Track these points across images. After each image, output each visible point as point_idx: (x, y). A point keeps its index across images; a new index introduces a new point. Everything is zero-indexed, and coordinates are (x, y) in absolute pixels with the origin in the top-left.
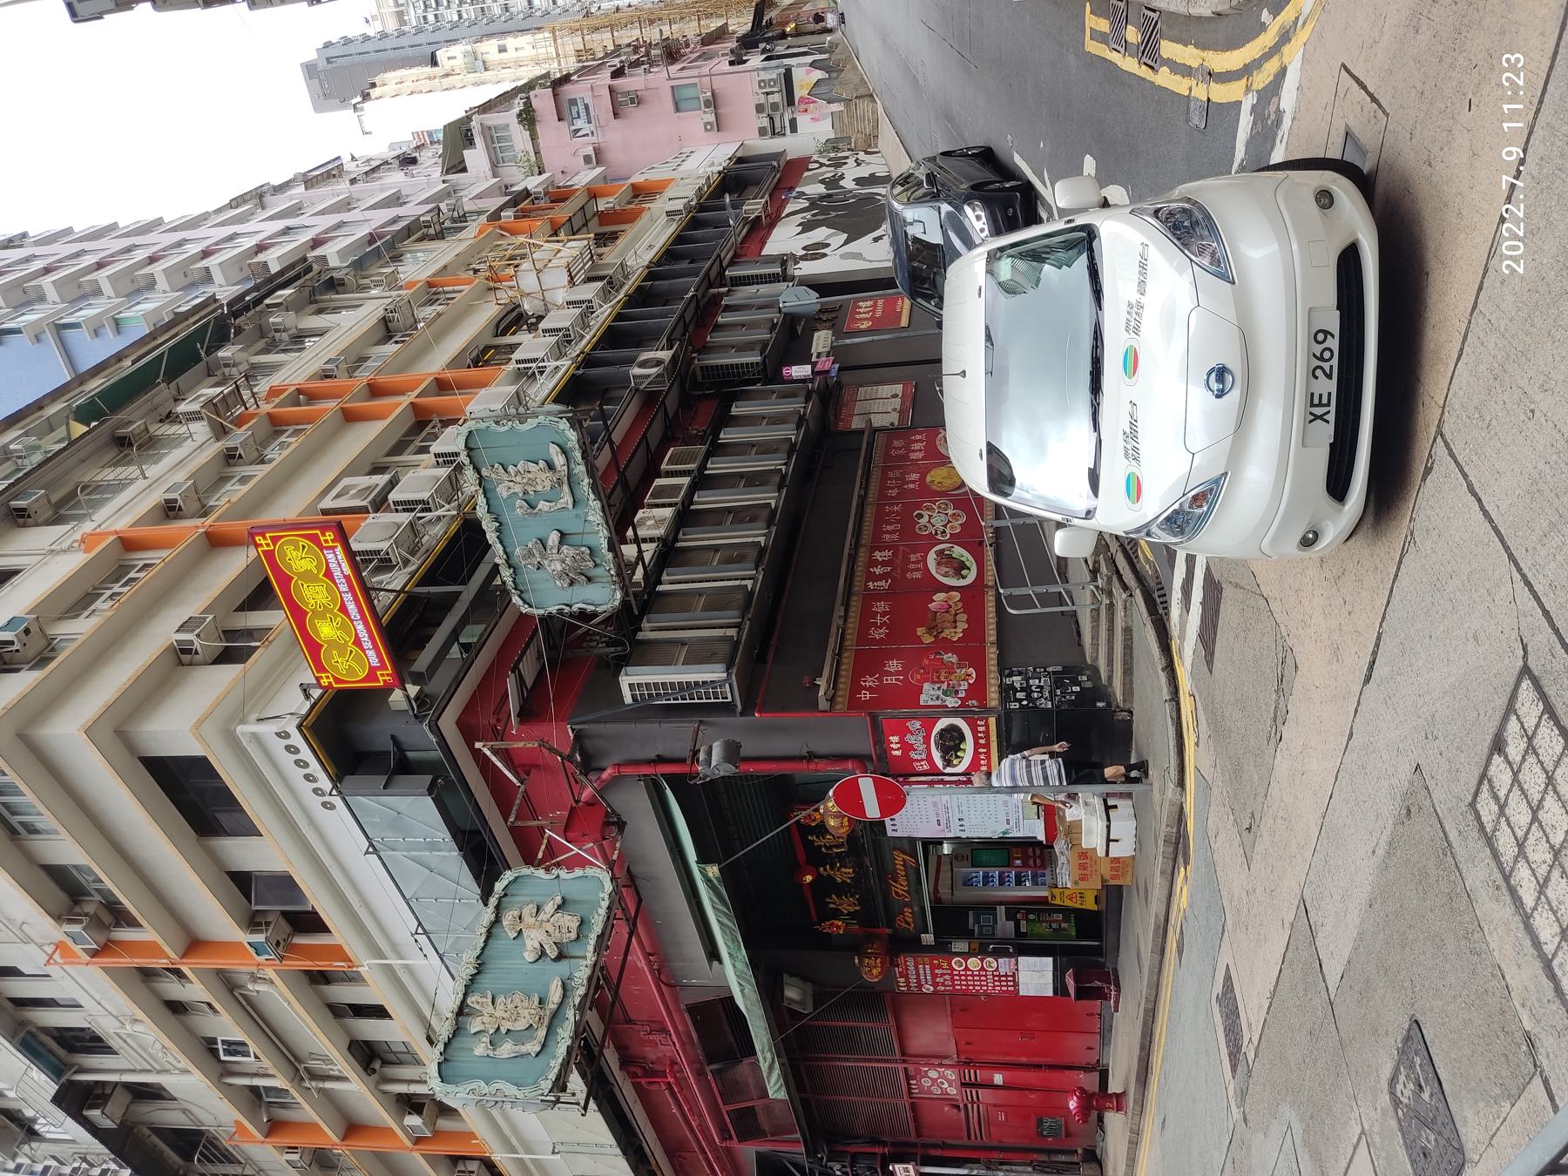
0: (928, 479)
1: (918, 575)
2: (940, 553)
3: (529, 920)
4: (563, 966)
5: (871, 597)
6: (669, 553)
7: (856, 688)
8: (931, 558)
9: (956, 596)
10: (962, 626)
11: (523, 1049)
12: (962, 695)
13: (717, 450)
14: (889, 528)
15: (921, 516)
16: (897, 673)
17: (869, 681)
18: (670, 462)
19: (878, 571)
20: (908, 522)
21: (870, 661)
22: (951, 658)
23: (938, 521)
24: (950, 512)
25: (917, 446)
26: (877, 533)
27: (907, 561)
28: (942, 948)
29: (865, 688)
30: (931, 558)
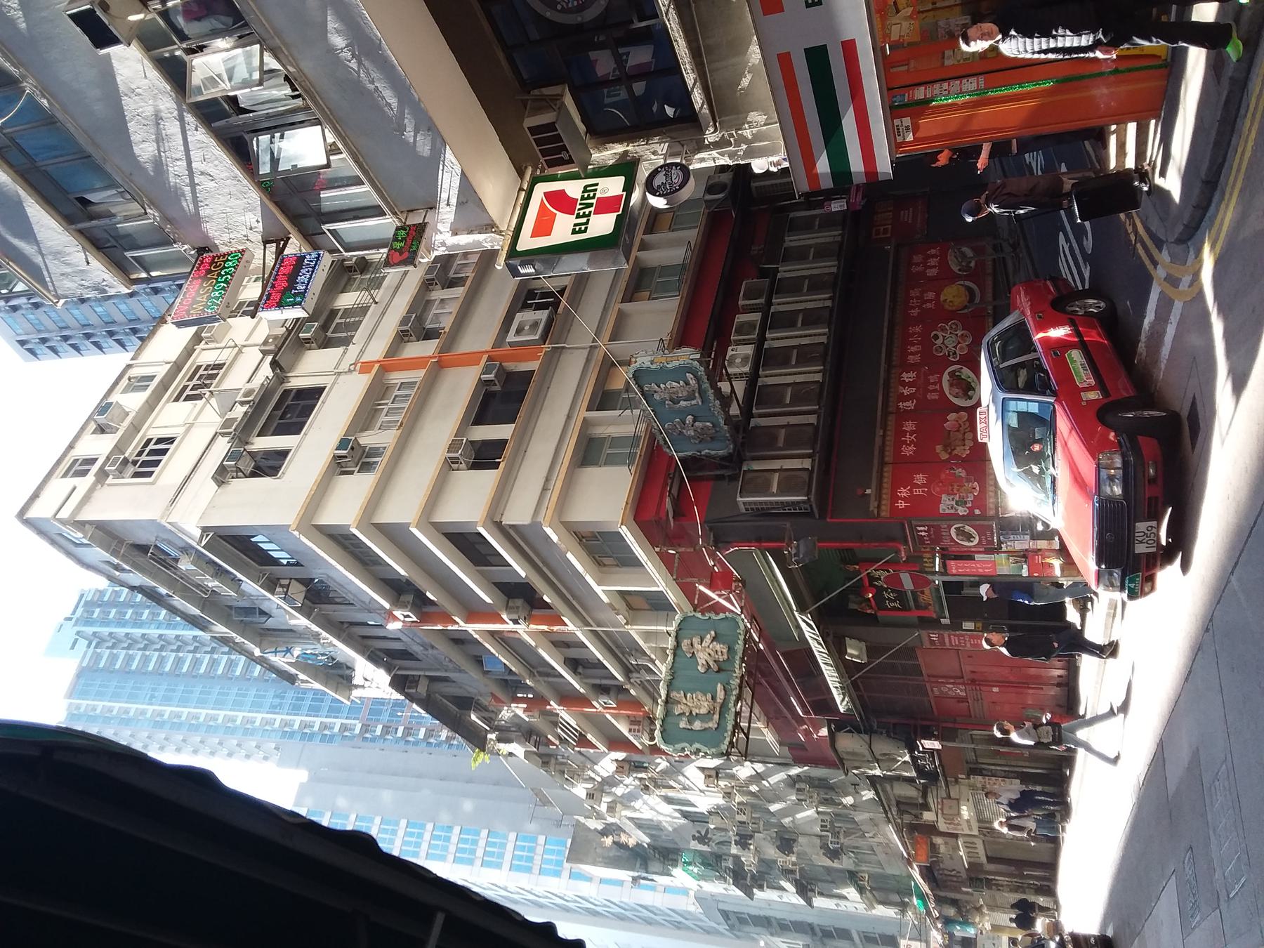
0: (942, 298)
1: (935, 396)
2: (952, 374)
3: (697, 646)
4: (722, 675)
6: (756, 394)
7: (895, 498)
8: (946, 377)
11: (706, 726)
13: (778, 287)
14: (913, 349)
15: (936, 337)
16: (923, 486)
17: (903, 493)
18: (746, 297)
19: (906, 392)
20: (927, 342)
22: (961, 472)
23: (950, 343)
25: (933, 262)
26: (905, 354)
27: (928, 383)
28: (956, 626)
30: (946, 377)
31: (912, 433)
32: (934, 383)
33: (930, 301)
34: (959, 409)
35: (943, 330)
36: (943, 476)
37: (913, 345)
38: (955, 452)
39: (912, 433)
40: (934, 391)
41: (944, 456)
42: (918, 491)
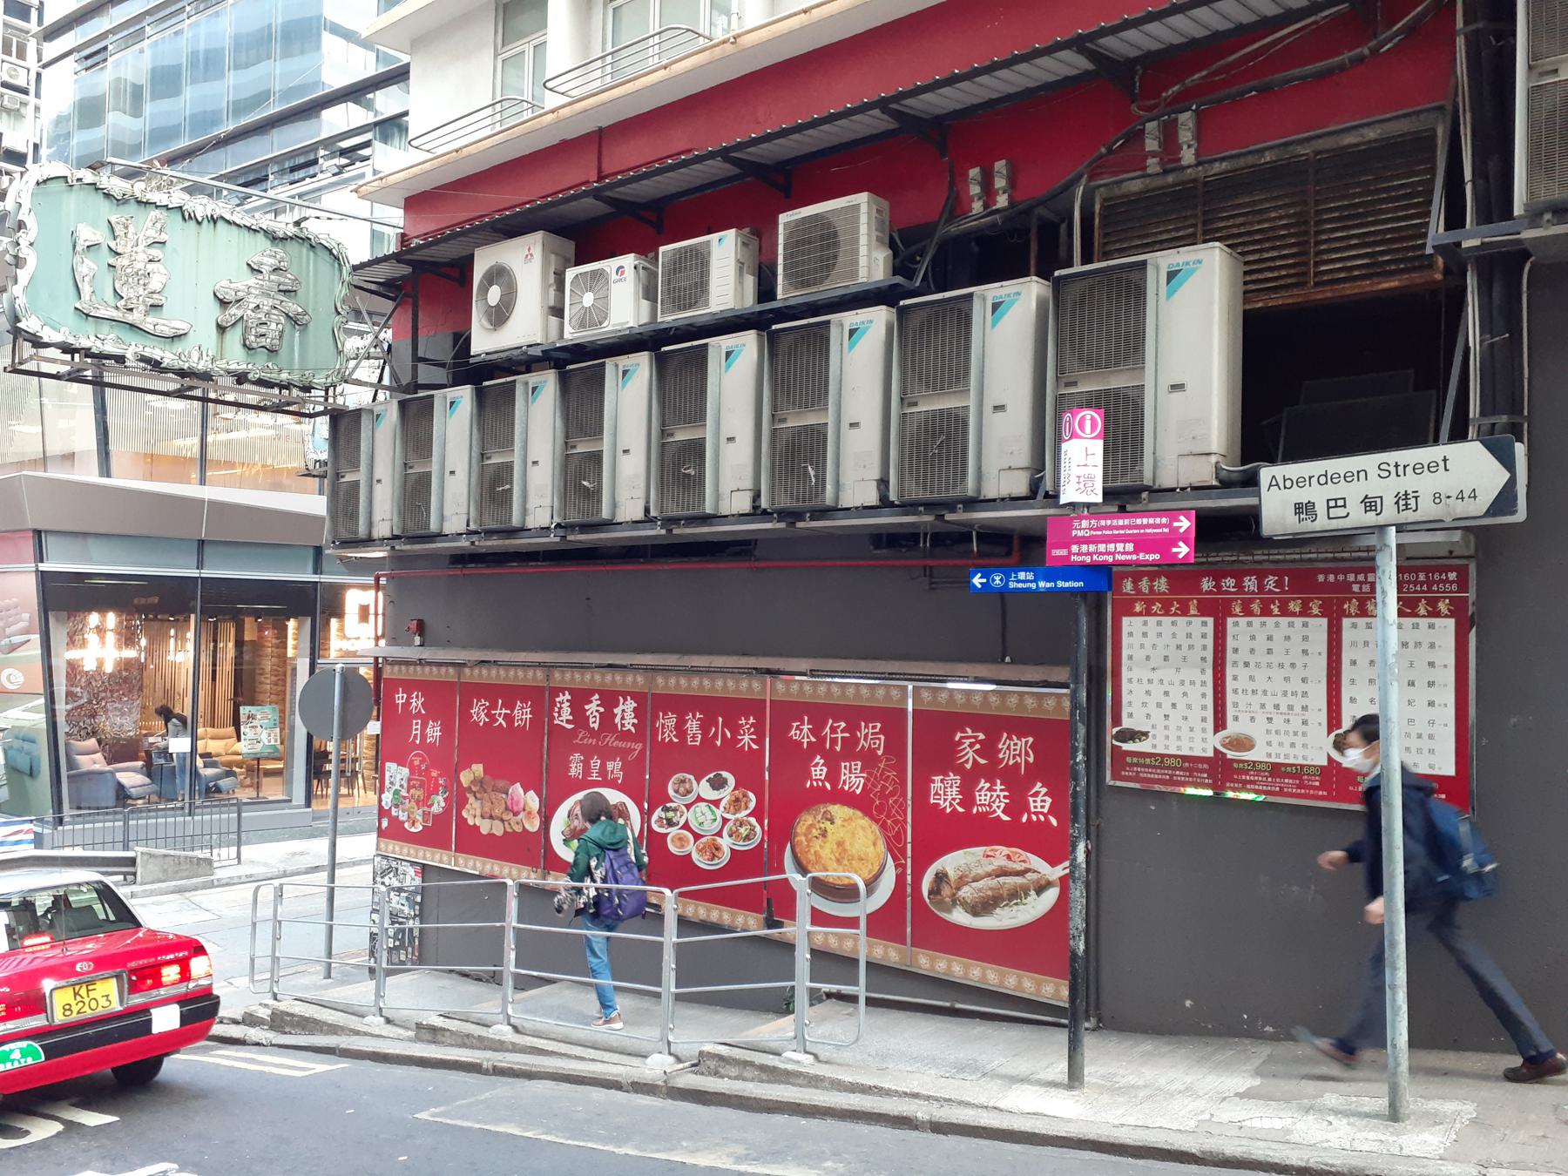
0: (839, 811)
1: (575, 770)
5: (541, 698)
7: (409, 686)
9: (534, 826)
10: (485, 827)
12: (394, 812)
14: (693, 726)
15: (718, 784)
16: (424, 736)
17: (417, 703)
19: (593, 708)
20: (703, 761)
21: (445, 698)
22: (438, 804)
23: (702, 818)
24: (725, 842)
27: (607, 754)
29: (409, 698)
31: (509, 718)
32: (603, 771)
33: (833, 776)
34: (547, 817)
35: (736, 803)
36: (434, 774)
37: (704, 727)
38: (471, 799)
39: (509, 718)
40: (587, 770)
41: (465, 778)
42: (416, 726)
